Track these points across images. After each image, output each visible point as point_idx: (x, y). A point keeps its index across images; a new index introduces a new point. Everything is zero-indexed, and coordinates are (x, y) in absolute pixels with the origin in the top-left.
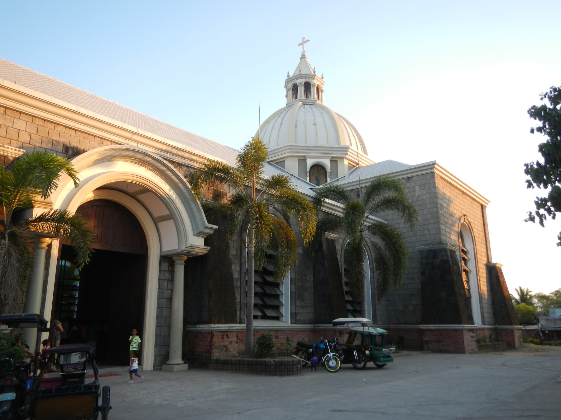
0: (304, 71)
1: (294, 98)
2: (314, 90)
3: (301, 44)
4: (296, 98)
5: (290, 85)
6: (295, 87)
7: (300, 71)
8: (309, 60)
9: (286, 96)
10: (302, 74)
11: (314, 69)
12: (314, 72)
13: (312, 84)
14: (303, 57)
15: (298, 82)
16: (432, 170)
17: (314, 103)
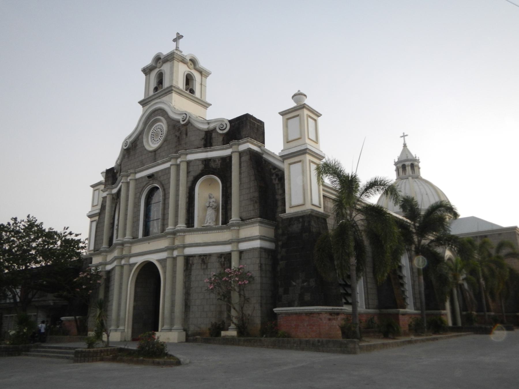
0: (410, 157)
1: (404, 174)
2: (416, 168)
3: (401, 137)
4: (405, 174)
5: (400, 165)
6: (404, 167)
7: (407, 157)
8: (409, 147)
9: (396, 170)
10: (409, 159)
11: (415, 155)
12: (416, 157)
13: (415, 165)
14: (405, 145)
15: (407, 163)
16: (514, 231)
17: (417, 177)
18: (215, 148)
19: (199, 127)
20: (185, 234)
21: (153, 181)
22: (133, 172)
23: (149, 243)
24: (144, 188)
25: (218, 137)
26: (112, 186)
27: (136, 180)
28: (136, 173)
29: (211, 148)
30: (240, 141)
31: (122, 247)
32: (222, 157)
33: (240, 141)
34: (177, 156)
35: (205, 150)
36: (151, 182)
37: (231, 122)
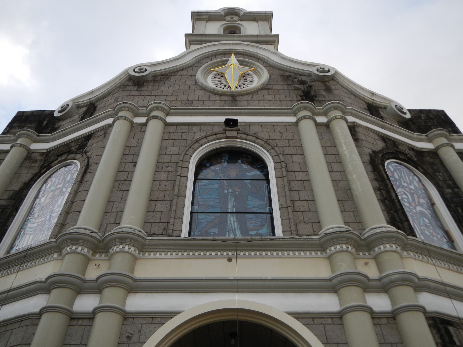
18: (400, 130)
19: (356, 90)
20: (405, 253)
21: (238, 133)
22: (167, 108)
23: (230, 260)
24: (205, 140)
25: (391, 120)
26: (38, 136)
27: (166, 124)
28: (168, 114)
29: (393, 126)
30: (453, 135)
31: (90, 254)
32: (412, 147)
33: (453, 135)
34: (316, 110)
35: (381, 123)
36: (229, 134)
37: (410, 111)
